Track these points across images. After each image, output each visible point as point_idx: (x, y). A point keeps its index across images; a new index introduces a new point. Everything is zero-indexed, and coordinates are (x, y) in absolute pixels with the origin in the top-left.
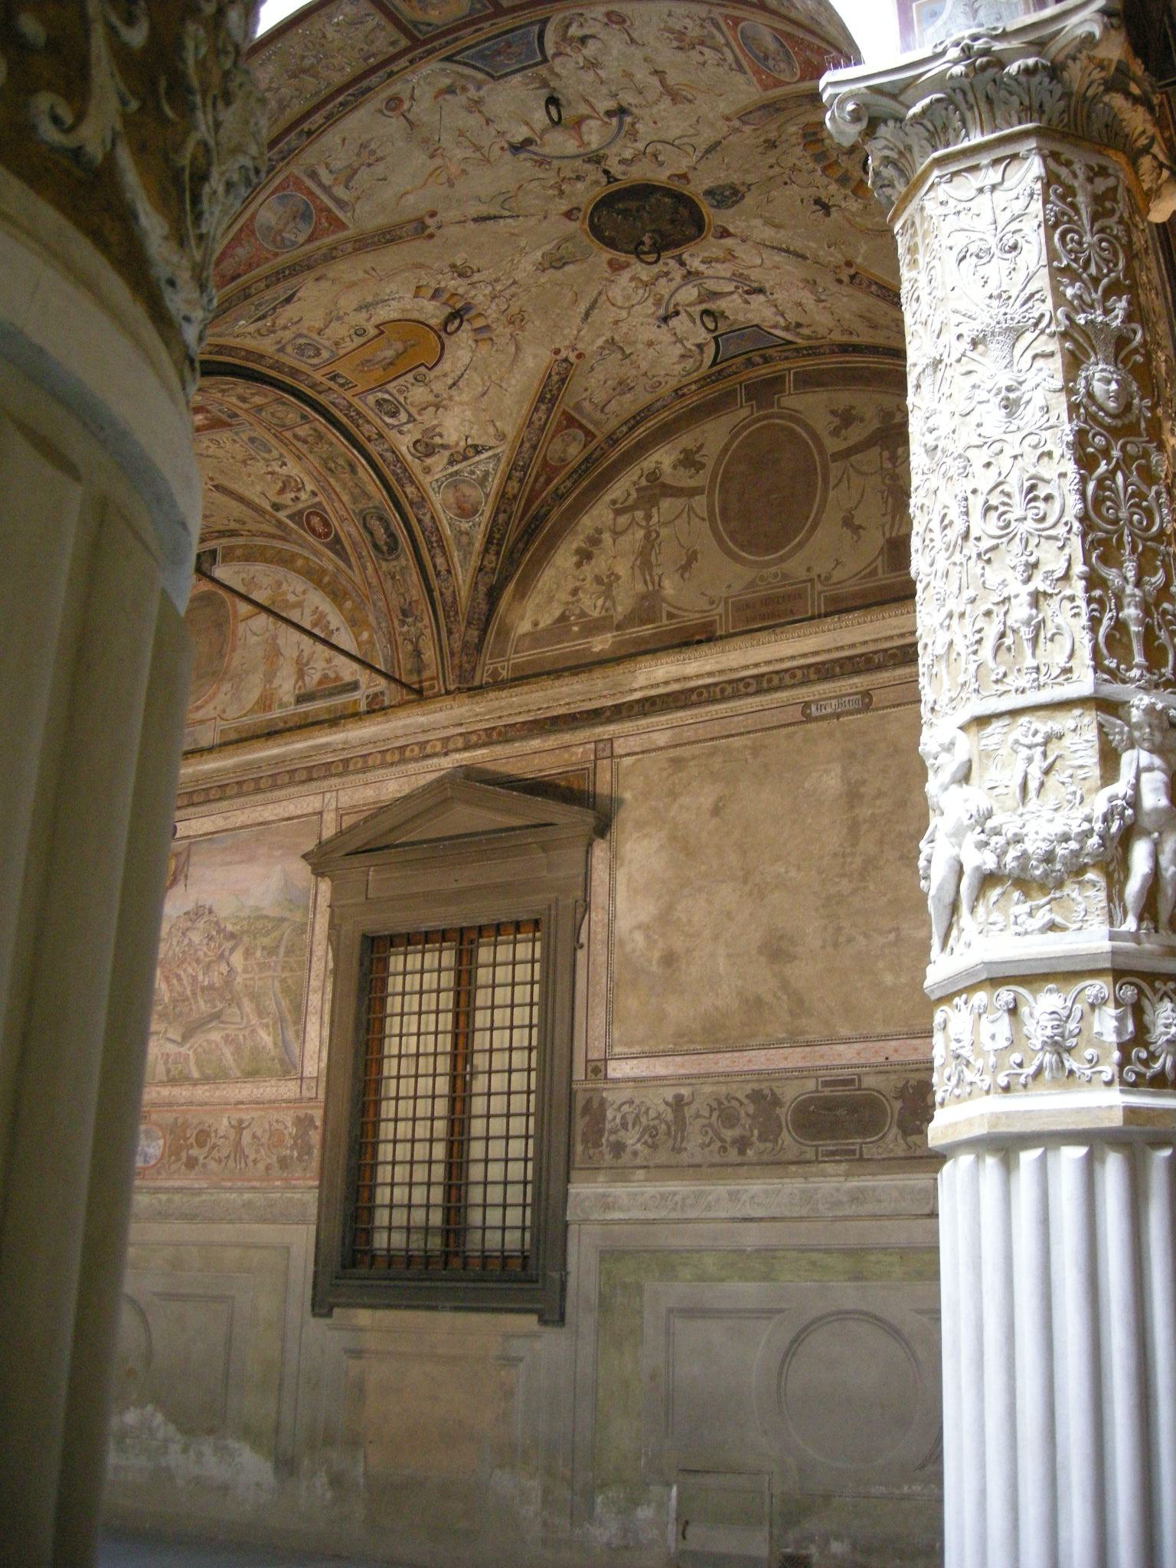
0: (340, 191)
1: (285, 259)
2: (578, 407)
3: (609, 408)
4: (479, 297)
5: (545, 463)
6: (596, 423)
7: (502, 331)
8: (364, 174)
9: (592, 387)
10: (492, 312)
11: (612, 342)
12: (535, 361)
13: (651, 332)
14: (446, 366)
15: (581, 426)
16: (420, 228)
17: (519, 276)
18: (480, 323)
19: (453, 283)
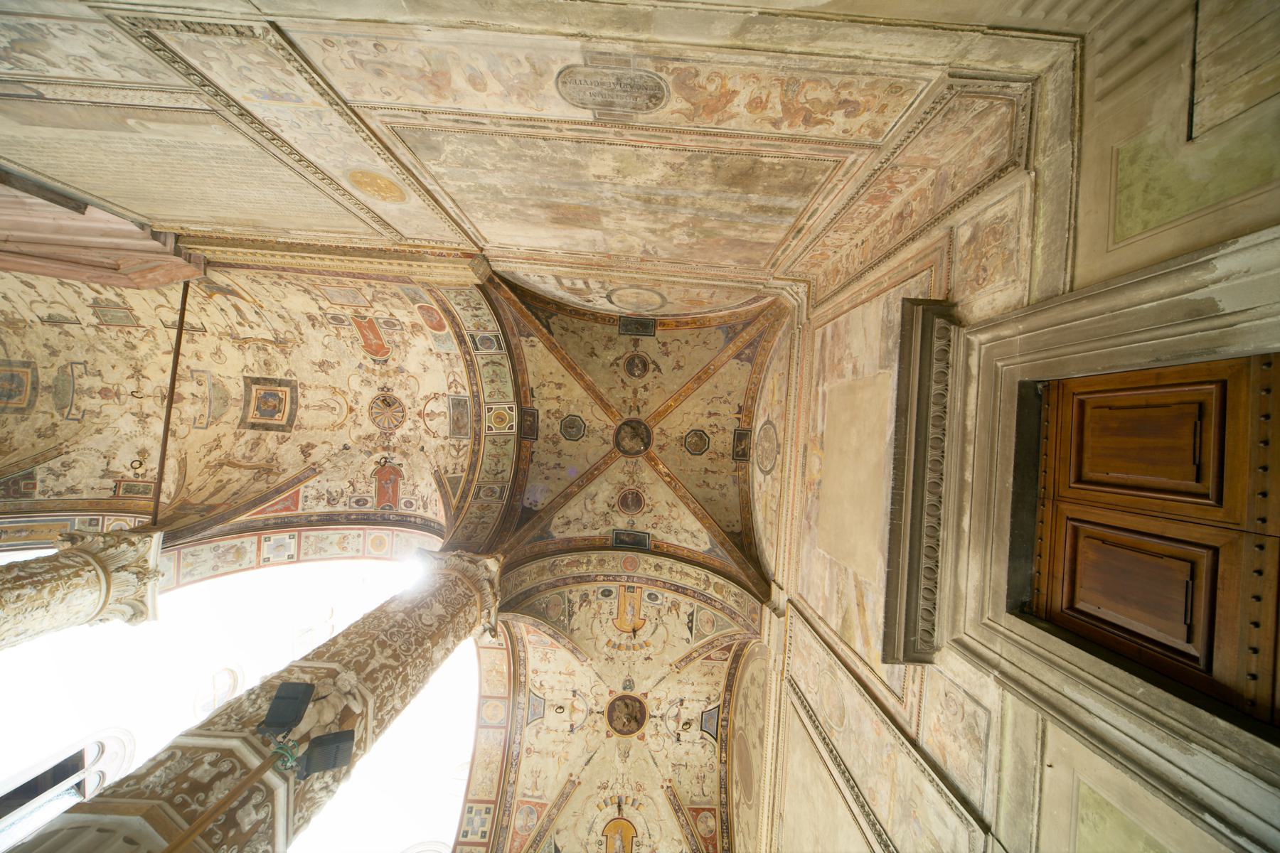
0: (537, 794)
1: (533, 834)
2: (692, 802)
3: (706, 791)
4: (619, 791)
5: (704, 839)
6: (709, 803)
7: (640, 797)
8: (539, 781)
9: (689, 789)
10: (630, 793)
11: (674, 765)
12: (661, 797)
13: (681, 749)
14: (640, 831)
15: (704, 810)
16: (573, 784)
17: (621, 771)
18: (630, 801)
19: (606, 794)
